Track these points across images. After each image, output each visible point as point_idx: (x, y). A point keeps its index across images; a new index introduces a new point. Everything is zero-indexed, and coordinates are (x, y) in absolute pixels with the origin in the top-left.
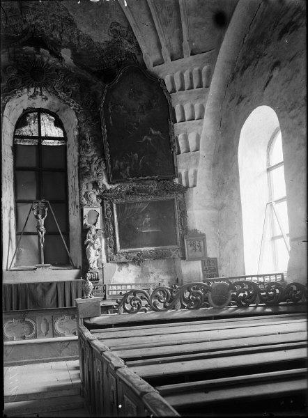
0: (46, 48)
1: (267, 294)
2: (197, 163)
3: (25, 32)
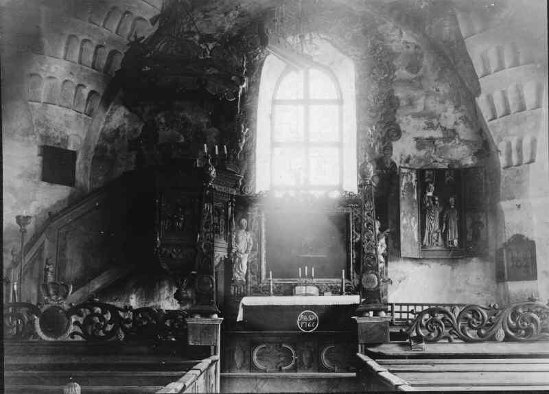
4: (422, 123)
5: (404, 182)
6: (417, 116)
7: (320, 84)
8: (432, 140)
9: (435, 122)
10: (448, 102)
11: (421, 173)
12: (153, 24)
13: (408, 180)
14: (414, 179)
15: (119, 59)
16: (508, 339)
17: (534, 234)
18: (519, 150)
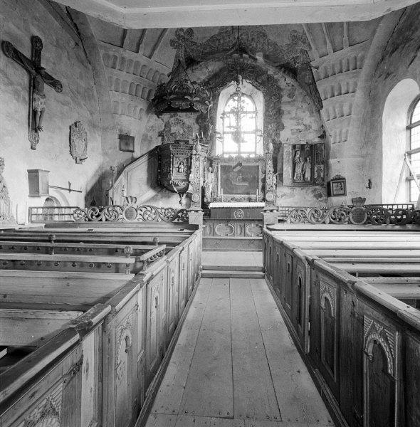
0: (246, 53)
1: (396, 217)
2: (349, 124)
3: (234, 45)
5: (285, 150)
6: (291, 119)
7: (248, 104)
10: (307, 112)
11: (294, 147)
12: (169, 76)
13: (287, 150)
14: (291, 147)
15: (153, 93)
16: (331, 223)
17: (343, 175)
18: (340, 135)
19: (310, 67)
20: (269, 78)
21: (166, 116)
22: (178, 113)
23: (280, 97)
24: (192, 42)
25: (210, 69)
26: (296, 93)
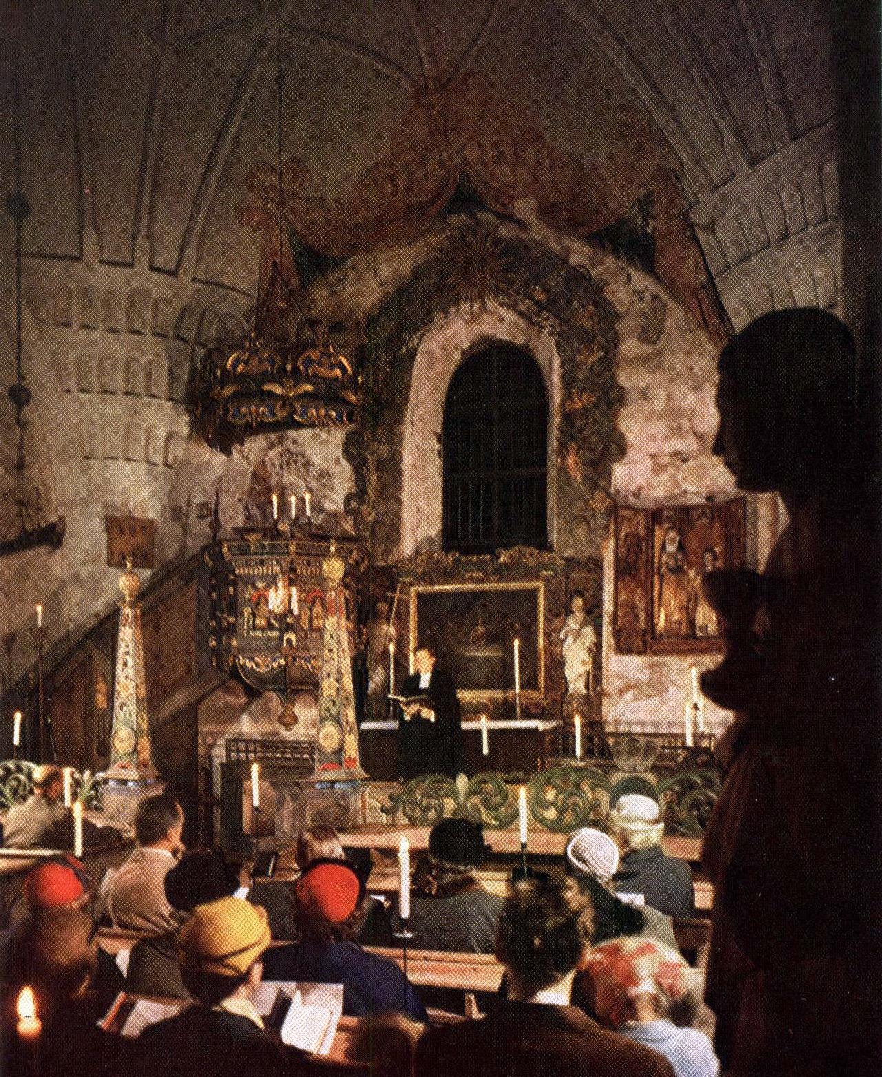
0: (484, 208)
3: (444, 184)
4: (661, 428)
6: (652, 417)
8: (681, 457)
9: (685, 424)
19: (691, 228)
20: (577, 277)
21: (255, 446)
22: (292, 433)
23: (614, 342)
24: (309, 199)
25: (385, 272)
26: (669, 324)
